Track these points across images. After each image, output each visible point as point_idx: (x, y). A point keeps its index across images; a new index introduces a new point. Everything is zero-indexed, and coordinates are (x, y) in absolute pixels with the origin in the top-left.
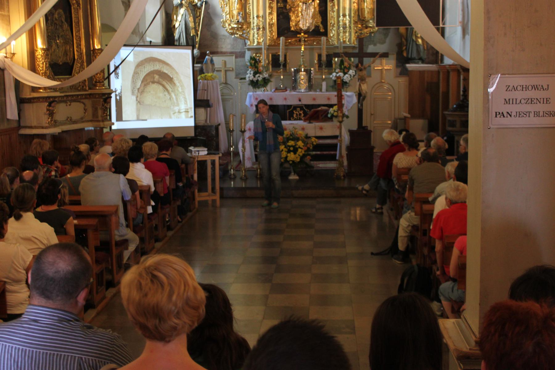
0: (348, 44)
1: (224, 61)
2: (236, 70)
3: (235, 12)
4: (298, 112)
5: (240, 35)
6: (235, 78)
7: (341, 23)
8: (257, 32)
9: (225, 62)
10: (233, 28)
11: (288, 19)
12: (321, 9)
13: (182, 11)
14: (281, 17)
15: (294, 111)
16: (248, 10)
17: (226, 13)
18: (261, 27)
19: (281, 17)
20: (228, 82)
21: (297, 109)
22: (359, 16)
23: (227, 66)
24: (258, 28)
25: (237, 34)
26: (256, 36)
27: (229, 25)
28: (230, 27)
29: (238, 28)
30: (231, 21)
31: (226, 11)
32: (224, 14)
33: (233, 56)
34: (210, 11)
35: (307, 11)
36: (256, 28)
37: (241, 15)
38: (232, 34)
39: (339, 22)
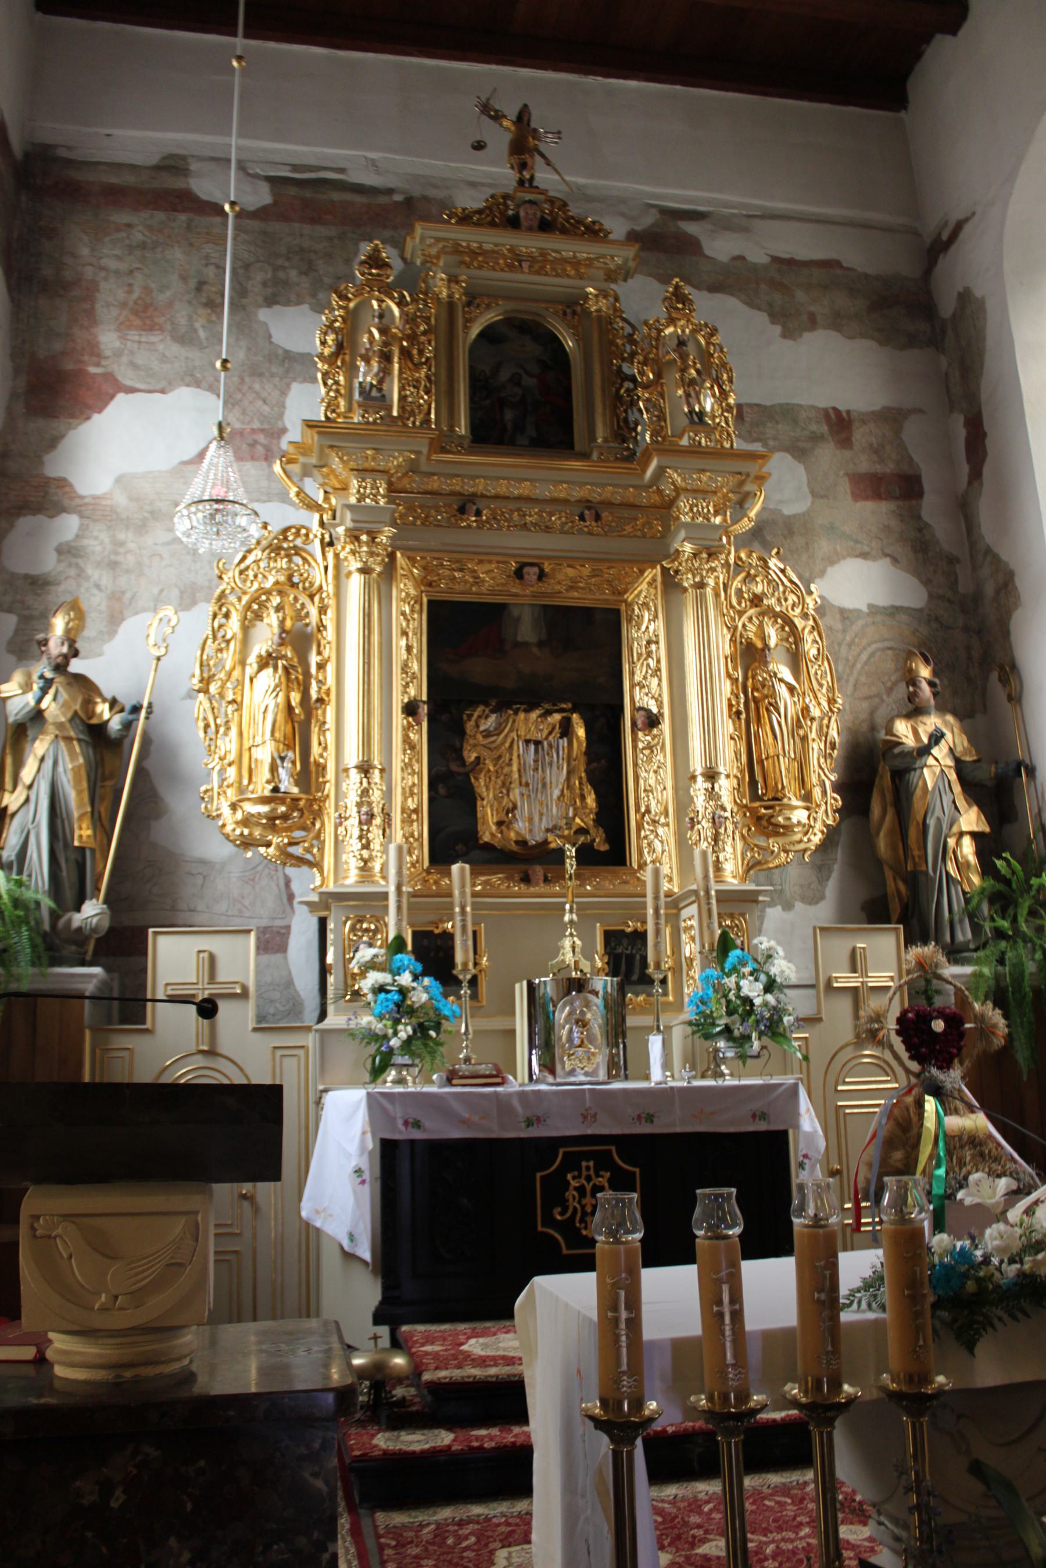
0: (733, 885)
1: (206, 955)
2: (259, 996)
3: (264, 754)
4: (588, 1179)
5: (283, 851)
6: (255, 1030)
7: (700, 801)
8: (362, 830)
9: (212, 959)
10: (246, 822)
11: (469, 799)
12: (595, 765)
13: (40, 746)
14: (442, 791)
15: (569, 1176)
16: (315, 750)
17: (221, 759)
18: (376, 810)
19: (442, 791)
20: (224, 1048)
21: (584, 1164)
22: (753, 783)
23: (221, 977)
24: (367, 813)
25: (268, 845)
26: (355, 845)
27: (234, 807)
28: (239, 815)
29: (272, 818)
30: (241, 790)
31: (222, 754)
32: (215, 763)
33: (249, 931)
34: (149, 764)
35: (543, 771)
36: (355, 814)
37: (287, 764)
38: (247, 843)
39: (683, 801)
